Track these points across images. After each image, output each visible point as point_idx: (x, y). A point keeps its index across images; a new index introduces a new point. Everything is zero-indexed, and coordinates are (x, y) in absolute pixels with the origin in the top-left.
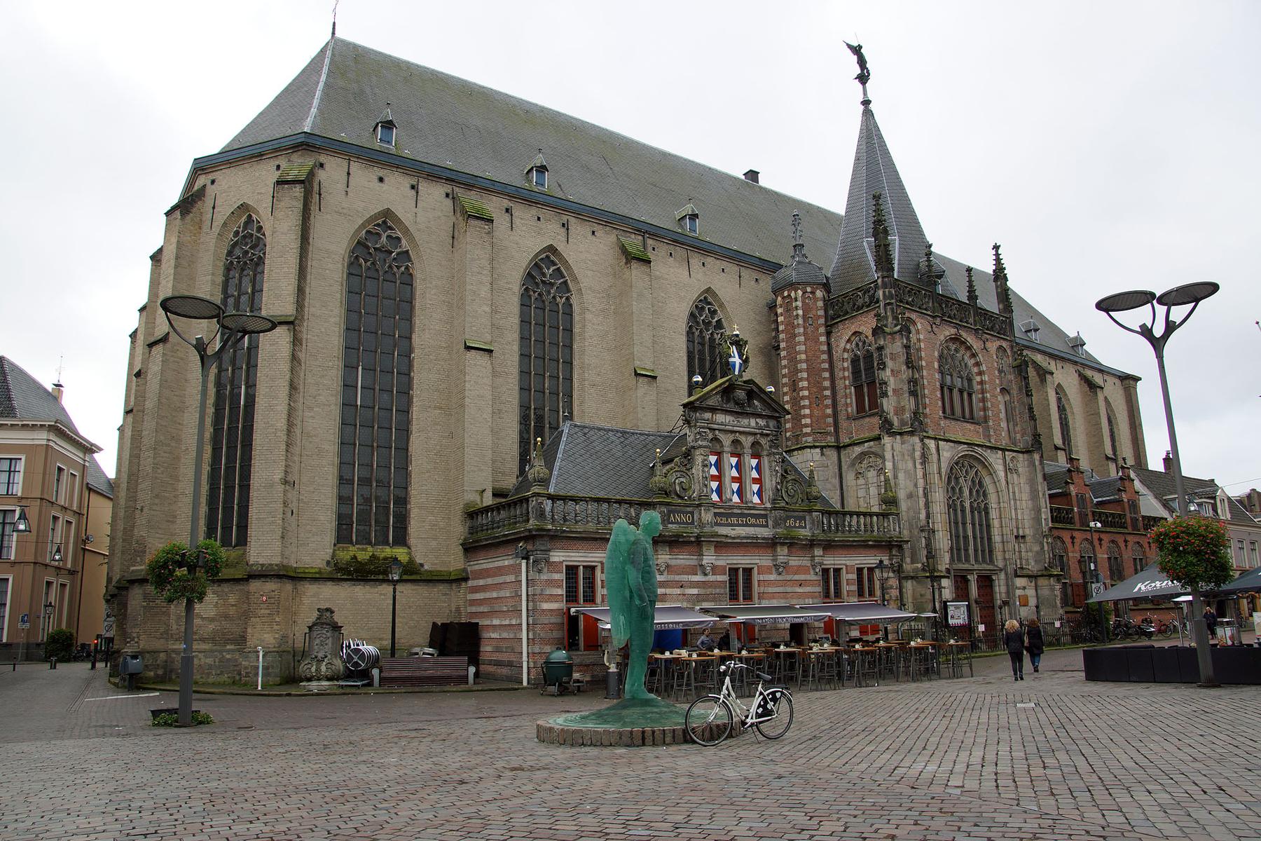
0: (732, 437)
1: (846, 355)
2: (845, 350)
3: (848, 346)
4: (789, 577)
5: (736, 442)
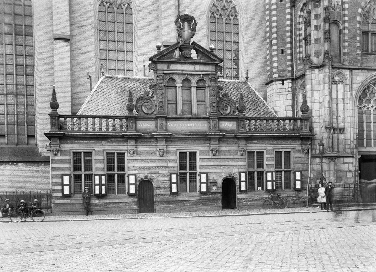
0: (182, 78)
1: (301, 20)
2: (300, 16)
3: (302, 13)
4: (222, 157)
5: (186, 80)
